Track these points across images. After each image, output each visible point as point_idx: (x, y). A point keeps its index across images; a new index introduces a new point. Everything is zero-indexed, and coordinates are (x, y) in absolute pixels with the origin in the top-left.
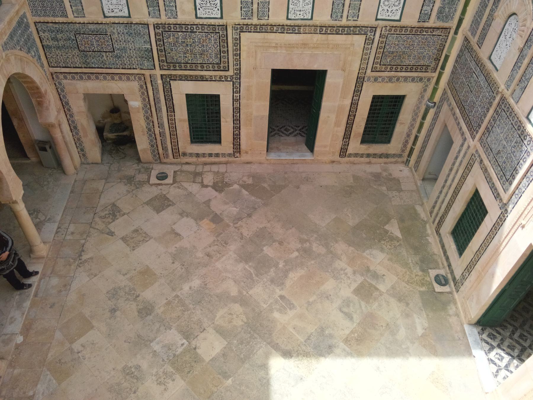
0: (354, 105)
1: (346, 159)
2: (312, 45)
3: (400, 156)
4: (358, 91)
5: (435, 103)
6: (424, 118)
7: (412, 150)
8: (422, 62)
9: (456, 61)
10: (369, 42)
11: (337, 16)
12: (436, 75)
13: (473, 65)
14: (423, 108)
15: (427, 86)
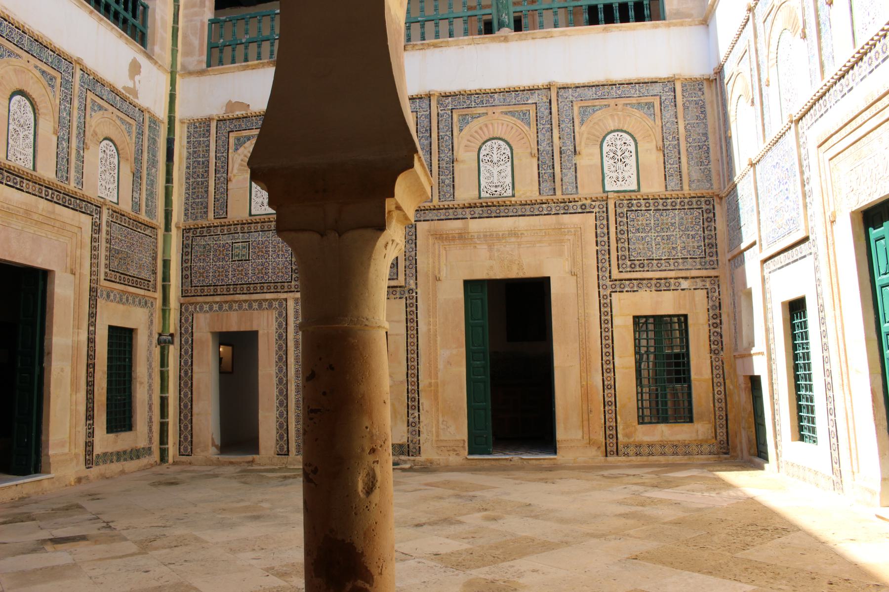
0: (91, 341)
1: (95, 471)
2: (35, 217)
3: (148, 451)
4: (92, 315)
5: (172, 335)
6: (164, 362)
7: (164, 427)
8: (143, 275)
9: (183, 261)
10: (96, 228)
11: (62, 176)
12: (159, 295)
13: (226, 240)
14: (157, 351)
15: (152, 314)
